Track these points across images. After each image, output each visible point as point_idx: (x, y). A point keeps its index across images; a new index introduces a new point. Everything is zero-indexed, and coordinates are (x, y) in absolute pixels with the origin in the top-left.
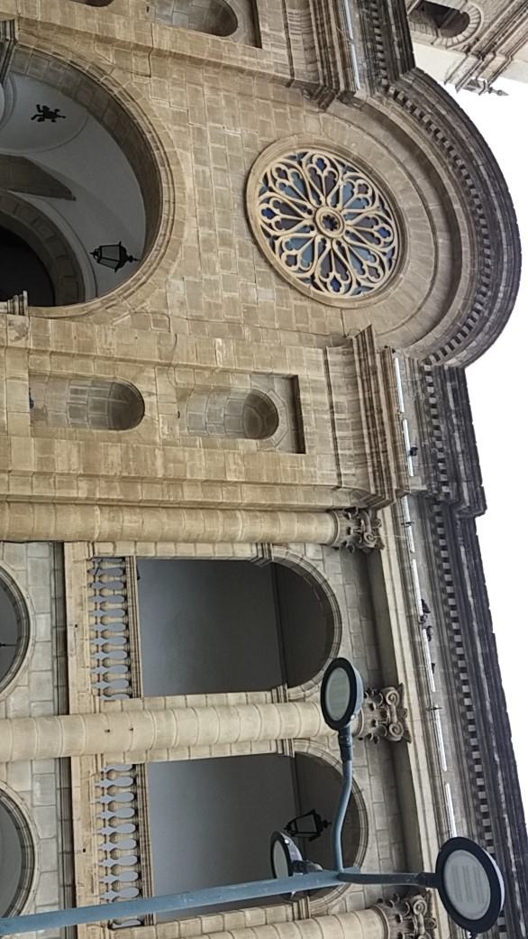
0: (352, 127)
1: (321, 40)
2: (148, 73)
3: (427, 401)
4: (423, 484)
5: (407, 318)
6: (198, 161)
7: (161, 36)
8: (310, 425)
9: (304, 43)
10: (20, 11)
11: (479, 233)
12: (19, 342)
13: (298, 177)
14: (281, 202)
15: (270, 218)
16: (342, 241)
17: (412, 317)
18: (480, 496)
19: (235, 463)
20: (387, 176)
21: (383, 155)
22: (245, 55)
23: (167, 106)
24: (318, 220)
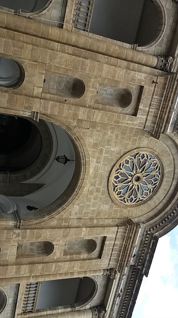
0: (160, 141)
1: (161, 114)
2: (88, 128)
3: (145, 242)
5: (151, 209)
6: (97, 162)
7: (98, 115)
8: (105, 250)
9: (154, 113)
12: (17, 238)
15: (116, 179)
17: (153, 209)
18: (147, 273)
19: (77, 265)
20: (165, 160)
22: (128, 120)
23: (92, 141)
24: (133, 179)
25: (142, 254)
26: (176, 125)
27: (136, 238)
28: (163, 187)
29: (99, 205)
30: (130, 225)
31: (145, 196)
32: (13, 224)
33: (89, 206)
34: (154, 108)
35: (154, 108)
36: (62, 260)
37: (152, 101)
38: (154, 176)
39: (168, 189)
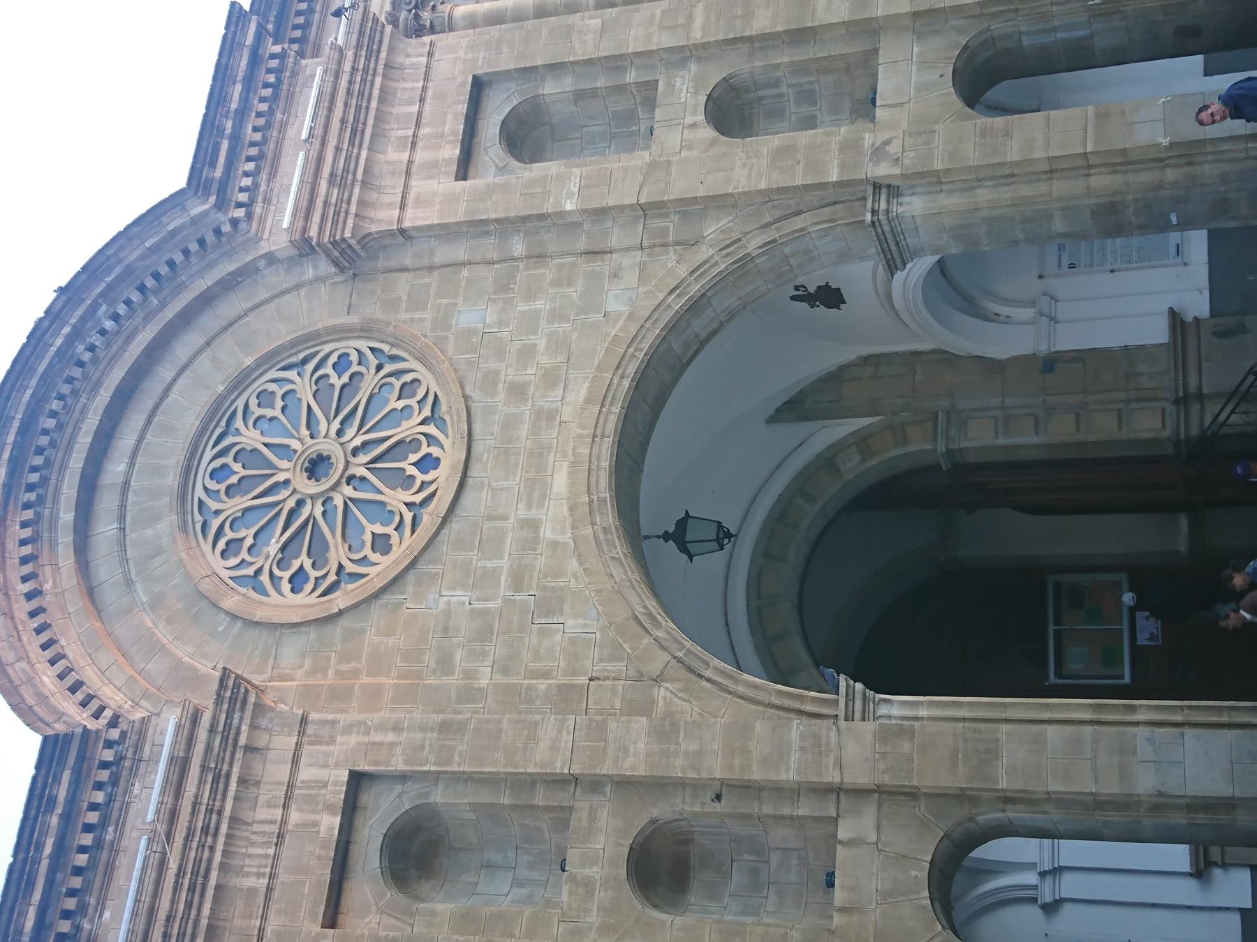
1: (219, 797)
4: (306, 66)
7: (554, 748)
8: (456, 115)
10: (833, 734)
11: (48, 463)
13: (350, 549)
14: (399, 489)
15: (428, 455)
16: (309, 441)
17: (225, 329)
18: (234, 19)
19: (585, 42)
21: (169, 621)
22: (393, 745)
23: (570, 622)
24: (341, 466)
25: (266, 109)
26: (129, 754)
27: (302, 182)
28: (181, 442)
29: (505, 327)
30: (343, 240)
31: (272, 387)
32: (908, 204)
33: (557, 315)
34: (256, 828)
35: (256, 828)
36: (661, 60)
37: (270, 861)
38: (232, 491)
39: (148, 436)
